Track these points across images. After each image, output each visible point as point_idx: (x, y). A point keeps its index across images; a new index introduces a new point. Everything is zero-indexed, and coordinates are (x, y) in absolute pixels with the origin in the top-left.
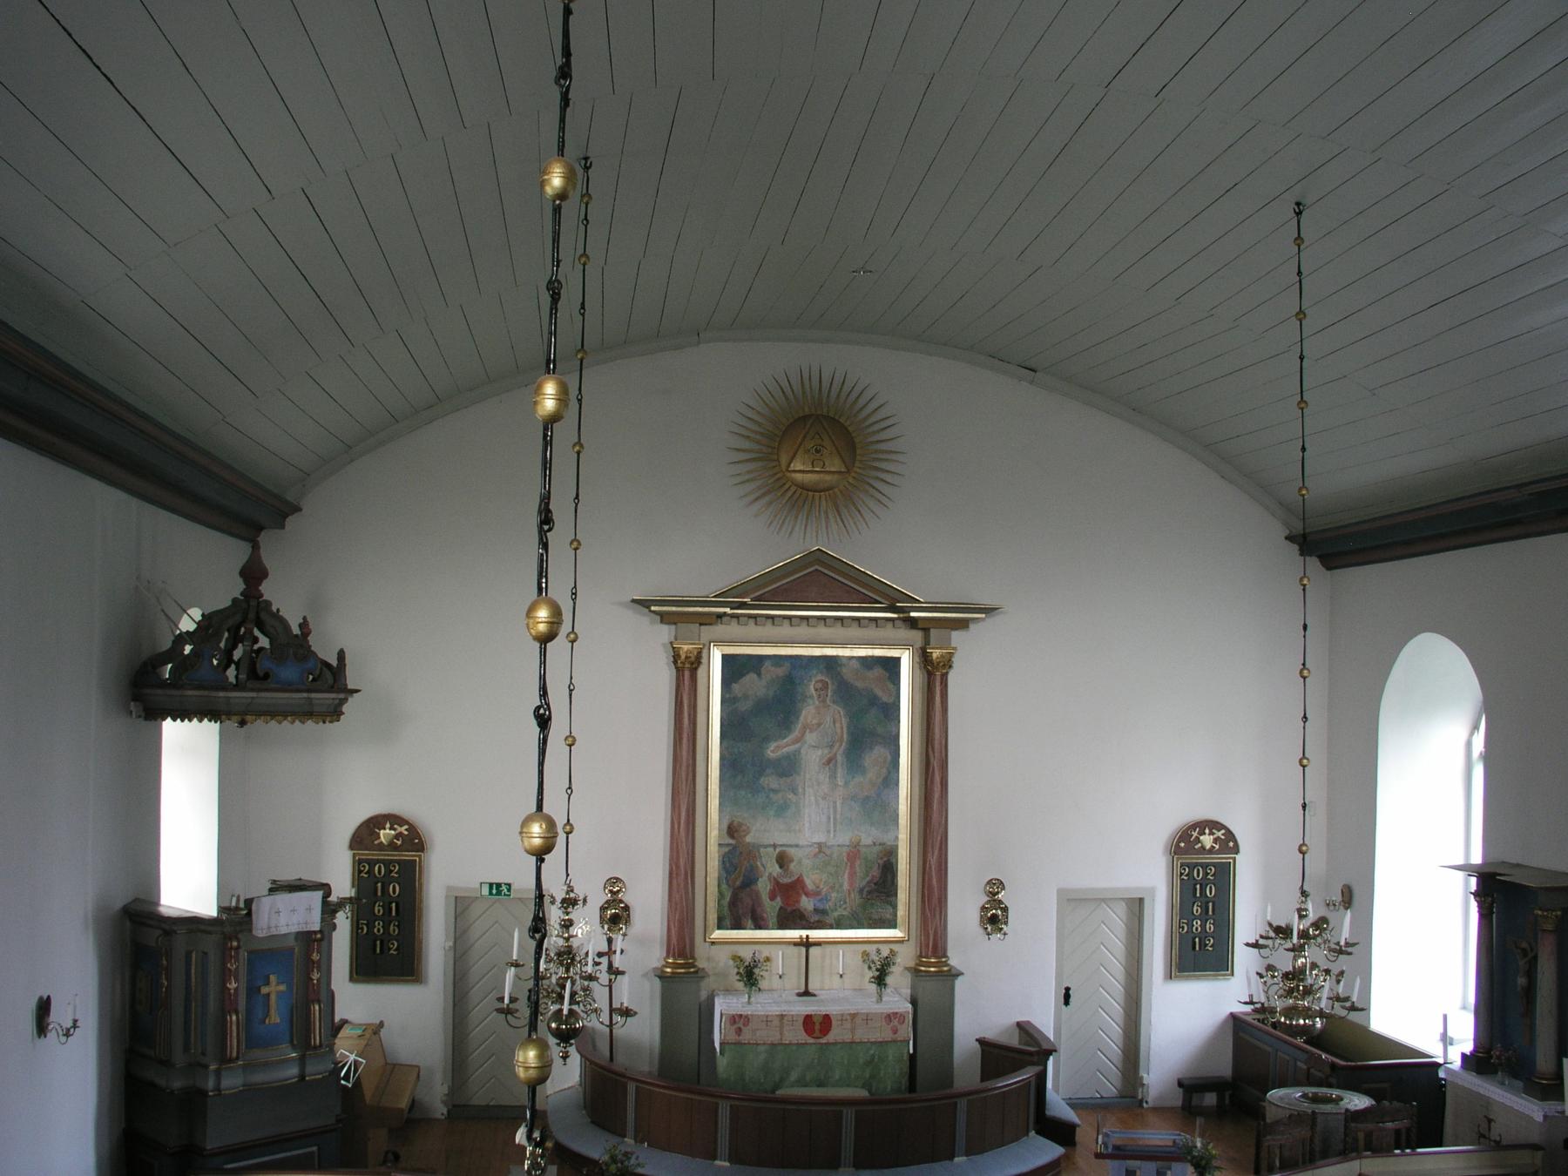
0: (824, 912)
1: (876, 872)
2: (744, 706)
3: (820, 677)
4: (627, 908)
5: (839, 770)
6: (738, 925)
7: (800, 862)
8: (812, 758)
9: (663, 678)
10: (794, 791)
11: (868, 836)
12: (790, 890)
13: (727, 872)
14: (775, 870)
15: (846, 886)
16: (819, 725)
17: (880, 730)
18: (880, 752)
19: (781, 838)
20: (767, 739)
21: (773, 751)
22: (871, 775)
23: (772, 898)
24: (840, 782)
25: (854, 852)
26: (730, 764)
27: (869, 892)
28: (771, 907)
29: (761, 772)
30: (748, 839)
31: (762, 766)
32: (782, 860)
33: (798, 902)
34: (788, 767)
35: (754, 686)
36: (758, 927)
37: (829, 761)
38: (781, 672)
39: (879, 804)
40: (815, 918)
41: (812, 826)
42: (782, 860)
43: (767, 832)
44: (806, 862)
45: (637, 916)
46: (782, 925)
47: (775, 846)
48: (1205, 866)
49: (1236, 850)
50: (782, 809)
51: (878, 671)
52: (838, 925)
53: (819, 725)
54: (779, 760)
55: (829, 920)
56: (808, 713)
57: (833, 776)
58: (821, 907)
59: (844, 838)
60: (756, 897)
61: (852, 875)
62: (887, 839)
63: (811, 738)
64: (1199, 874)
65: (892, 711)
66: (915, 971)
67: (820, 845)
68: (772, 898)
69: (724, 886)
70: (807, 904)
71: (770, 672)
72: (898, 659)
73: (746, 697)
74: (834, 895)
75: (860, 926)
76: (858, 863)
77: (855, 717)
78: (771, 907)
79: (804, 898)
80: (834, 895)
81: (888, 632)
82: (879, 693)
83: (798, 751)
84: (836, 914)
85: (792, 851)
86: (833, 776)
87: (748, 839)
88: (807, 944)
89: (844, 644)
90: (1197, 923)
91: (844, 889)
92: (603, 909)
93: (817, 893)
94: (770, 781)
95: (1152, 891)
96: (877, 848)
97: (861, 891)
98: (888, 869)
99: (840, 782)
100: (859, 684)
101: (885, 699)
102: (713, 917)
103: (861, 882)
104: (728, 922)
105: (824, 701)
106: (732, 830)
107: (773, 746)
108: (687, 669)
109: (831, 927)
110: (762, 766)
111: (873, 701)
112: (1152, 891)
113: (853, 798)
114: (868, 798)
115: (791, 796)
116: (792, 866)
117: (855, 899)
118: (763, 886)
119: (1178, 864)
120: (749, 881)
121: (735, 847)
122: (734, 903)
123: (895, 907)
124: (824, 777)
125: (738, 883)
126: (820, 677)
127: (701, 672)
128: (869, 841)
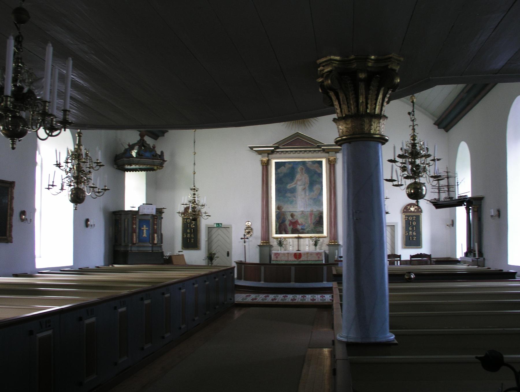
1: (317, 219)
2: (281, 175)
3: (301, 167)
4: (252, 229)
6: (281, 233)
8: (300, 188)
9: (260, 168)
10: (295, 197)
11: (315, 209)
12: (294, 223)
14: (290, 218)
15: (310, 222)
18: (318, 186)
19: (291, 210)
20: (287, 184)
21: (289, 186)
22: (316, 192)
28: (289, 228)
29: (286, 192)
30: (283, 210)
31: (286, 191)
32: (292, 216)
34: (293, 191)
35: (284, 170)
36: (286, 233)
38: (290, 166)
39: (318, 201)
40: (301, 231)
41: (300, 206)
43: (288, 208)
45: (254, 231)
46: (292, 233)
47: (290, 212)
48: (412, 216)
49: (421, 212)
50: (291, 202)
51: (316, 165)
52: (308, 233)
55: (305, 231)
56: (298, 176)
57: (305, 193)
59: (309, 209)
60: (285, 225)
61: (311, 219)
62: (320, 209)
63: (299, 183)
64: (410, 218)
65: (321, 175)
66: (329, 245)
70: (299, 227)
71: (287, 166)
72: (322, 161)
73: (281, 173)
77: (311, 177)
78: (289, 228)
79: (298, 226)
81: (320, 154)
83: (295, 187)
86: (305, 193)
87: (283, 210)
88: (299, 238)
89: (308, 158)
90: (411, 232)
91: (309, 223)
92: (245, 230)
93: (302, 224)
95: (397, 223)
97: (314, 223)
99: (307, 194)
101: (319, 172)
102: (274, 230)
103: (313, 221)
106: (278, 208)
107: (289, 185)
108: (266, 166)
109: (306, 233)
110: (286, 191)
111: (316, 173)
112: (397, 223)
113: (311, 198)
114: (315, 199)
115: (294, 198)
116: (295, 217)
117: (312, 226)
118: (287, 223)
119: (404, 216)
121: (279, 213)
123: (323, 228)
124: (303, 193)
126: (301, 167)
127: (269, 167)
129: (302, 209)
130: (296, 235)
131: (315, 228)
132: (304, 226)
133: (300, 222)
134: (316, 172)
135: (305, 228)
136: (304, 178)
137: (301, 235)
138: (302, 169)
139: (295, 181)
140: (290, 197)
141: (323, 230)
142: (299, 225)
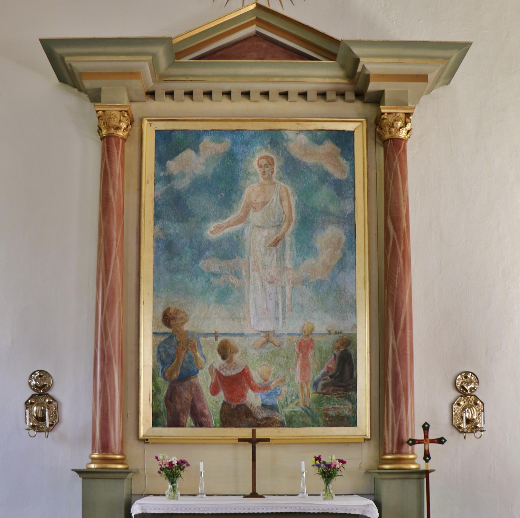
0: (273, 408)
1: (331, 363)
5: (288, 252)
6: (175, 423)
7: (245, 353)
10: (237, 275)
11: (322, 324)
12: (234, 384)
13: (163, 363)
14: (218, 361)
15: (298, 379)
16: (264, 203)
17: (332, 208)
21: (213, 231)
23: (214, 391)
24: (289, 264)
25: (306, 344)
26: (166, 247)
27: (325, 386)
28: (213, 403)
29: (200, 254)
30: (187, 327)
31: (201, 249)
32: (225, 351)
33: (243, 396)
34: (231, 249)
37: (276, 242)
40: (262, 414)
42: (225, 351)
44: (251, 352)
47: (216, 335)
53: (264, 203)
54: (220, 242)
55: (280, 416)
57: (281, 258)
58: (269, 401)
59: (294, 326)
60: (198, 389)
61: (305, 367)
62: (343, 327)
63: (255, 217)
67: (267, 334)
68: (214, 391)
69: (160, 379)
70: (253, 399)
74: (284, 389)
75: (316, 423)
76: (311, 353)
78: (213, 403)
80: (284, 389)
82: (330, 169)
84: (287, 410)
85: (235, 341)
86: (281, 258)
87: (187, 327)
93: (266, 388)
94: (210, 264)
96: (333, 338)
97: (315, 384)
98: (346, 361)
99: (289, 264)
100: (309, 161)
101: (337, 175)
104: (164, 419)
105: (269, 178)
106: (167, 318)
109: (282, 425)
110: (201, 249)
111: (325, 177)
113: (305, 282)
114: (320, 283)
115: (234, 280)
116: (236, 357)
117: (310, 394)
118: (204, 380)
120: (188, 375)
121: (171, 337)
122: (171, 397)
123: (354, 402)
124: (271, 259)
125: (175, 376)
128: (324, 330)
129: (266, 326)
130: (246, 432)
131: (318, 402)
132: (276, 393)
133: (256, 378)
134: (327, 174)
135: (277, 401)
136: (275, 198)
137: (261, 433)
138: (270, 163)
139: (238, 213)
140: (214, 274)
141: (355, 411)
142: (253, 388)
